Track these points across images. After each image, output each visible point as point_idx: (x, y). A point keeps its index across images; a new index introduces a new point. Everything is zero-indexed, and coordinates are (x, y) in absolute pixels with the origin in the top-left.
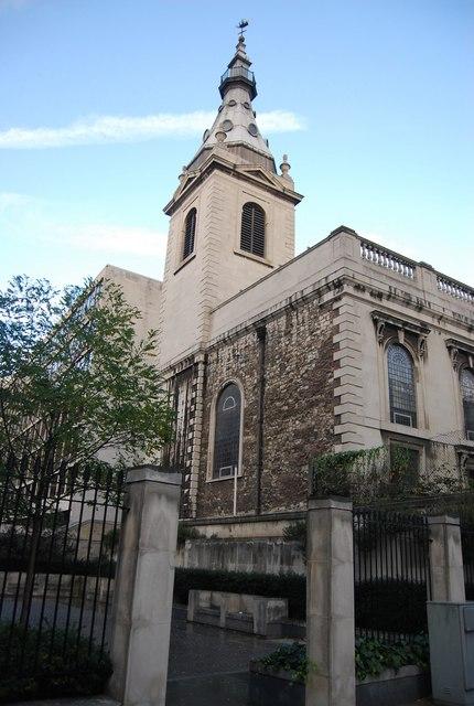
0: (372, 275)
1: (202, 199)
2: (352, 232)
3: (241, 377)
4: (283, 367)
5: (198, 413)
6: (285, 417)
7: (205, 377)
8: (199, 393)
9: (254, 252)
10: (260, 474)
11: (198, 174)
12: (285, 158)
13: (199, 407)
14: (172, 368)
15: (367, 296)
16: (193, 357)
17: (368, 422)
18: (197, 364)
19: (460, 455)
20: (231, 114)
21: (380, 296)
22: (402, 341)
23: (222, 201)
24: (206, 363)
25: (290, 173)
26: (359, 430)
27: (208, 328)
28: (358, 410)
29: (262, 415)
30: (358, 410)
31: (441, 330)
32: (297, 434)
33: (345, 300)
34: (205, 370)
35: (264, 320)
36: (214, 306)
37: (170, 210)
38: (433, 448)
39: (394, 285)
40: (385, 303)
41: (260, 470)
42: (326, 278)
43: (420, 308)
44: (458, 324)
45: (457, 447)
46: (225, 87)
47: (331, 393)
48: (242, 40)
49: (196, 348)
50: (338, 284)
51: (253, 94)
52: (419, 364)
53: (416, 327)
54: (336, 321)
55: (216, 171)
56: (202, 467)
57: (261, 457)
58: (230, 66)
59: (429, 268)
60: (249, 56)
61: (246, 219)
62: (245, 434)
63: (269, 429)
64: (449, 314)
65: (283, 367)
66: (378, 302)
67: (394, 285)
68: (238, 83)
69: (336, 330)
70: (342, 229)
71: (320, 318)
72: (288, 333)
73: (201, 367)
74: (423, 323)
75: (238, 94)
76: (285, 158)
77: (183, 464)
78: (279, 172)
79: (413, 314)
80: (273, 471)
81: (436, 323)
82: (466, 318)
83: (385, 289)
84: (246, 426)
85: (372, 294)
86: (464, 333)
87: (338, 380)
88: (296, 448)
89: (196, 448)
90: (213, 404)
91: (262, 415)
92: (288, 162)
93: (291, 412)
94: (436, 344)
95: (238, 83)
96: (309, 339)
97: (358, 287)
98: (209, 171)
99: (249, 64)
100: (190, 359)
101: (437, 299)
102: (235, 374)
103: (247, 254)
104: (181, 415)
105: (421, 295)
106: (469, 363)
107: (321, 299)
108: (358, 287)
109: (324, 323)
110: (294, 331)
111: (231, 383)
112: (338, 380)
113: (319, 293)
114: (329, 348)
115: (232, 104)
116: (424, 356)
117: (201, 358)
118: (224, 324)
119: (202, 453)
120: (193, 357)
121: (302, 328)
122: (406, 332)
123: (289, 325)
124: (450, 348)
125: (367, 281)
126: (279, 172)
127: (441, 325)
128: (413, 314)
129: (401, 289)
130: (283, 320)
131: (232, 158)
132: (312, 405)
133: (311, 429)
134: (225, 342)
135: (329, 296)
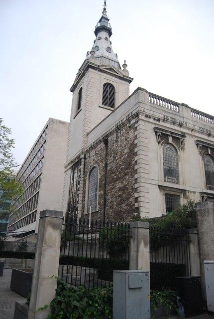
0: (155, 110)
1: (84, 84)
2: (144, 90)
3: (98, 164)
4: (115, 157)
5: (82, 182)
6: (115, 182)
7: (84, 165)
8: (82, 172)
9: (109, 106)
10: (105, 210)
11: (83, 72)
12: (125, 61)
13: (82, 179)
14: (72, 162)
15: (152, 120)
16: (80, 156)
17: (151, 182)
18: (81, 159)
19: (203, 197)
20: (99, 43)
21: (159, 120)
22: (170, 141)
23: (95, 82)
24: (85, 158)
25: (127, 68)
26: (146, 186)
27: (85, 142)
28: (146, 176)
29: (106, 181)
30: (146, 176)
32: (120, 189)
33: (140, 122)
34: (84, 162)
35: (107, 136)
36: (88, 132)
37: (72, 90)
38: (187, 194)
39: (166, 114)
40: (161, 123)
41: (105, 207)
42: (132, 113)
43: (181, 125)
44: (202, 132)
46: (97, 31)
47: (134, 168)
48: (105, 9)
49: (81, 151)
50: (137, 115)
51: (110, 34)
52: (180, 153)
53: (178, 135)
54: (136, 133)
55: (90, 69)
56: (83, 207)
57: (105, 201)
58: (100, 22)
59: (187, 106)
60: (108, 15)
61: (105, 91)
62: (100, 191)
63: (108, 187)
64: (197, 128)
65: (115, 157)
66: (158, 123)
67: (166, 114)
68: (103, 29)
69: (136, 137)
70: (139, 89)
71: (130, 132)
72: (117, 141)
73: (83, 160)
74: (182, 133)
75: (103, 34)
76: (125, 61)
78: (122, 68)
79: (176, 128)
80: (110, 208)
81: (190, 132)
82: (207, 130)
83: (161, 116)
84: (100, 187)
85: (154, 119)
86: (206, 137)
87: (137, 161)
88: (119, 196)
89: (80, 199)
90: (88, 177)
91: (106, 181)
92: (126, 63)
93: (118, 179)
94: (190, 143)
95: (103, 29)
96: (125, 143)
98: (87, 69)
99: (108, 20)
100: (79, 157)
101: (190, 119)
102: (96, 162)
103: (106, 107)
104: (75, 183)
105: (182, 119)
106: (208, 152)
107: (130, 123)
108: (146, 116)
110: (119, 140)
111: (94, 167)
112: (137, 161)
113: (129, 120)
114: (134, 146)
115: (100, 38)
117: (83, 156)
118: (92, 139)
119: (83, 201)
120: (80, 156)
121: (122, 138)
122: (173, 137)
123: (117, 137)
124: (197, 145)
125: (152, 112)
126: (122, 68)
127: (193, 133)
128: (176, 128)
129: (170, 116)
130: (115, 135)
131: (97, 62)
132: (126, 174)
133: (125, 186)
134: (92, 148)
135: (133, 121)
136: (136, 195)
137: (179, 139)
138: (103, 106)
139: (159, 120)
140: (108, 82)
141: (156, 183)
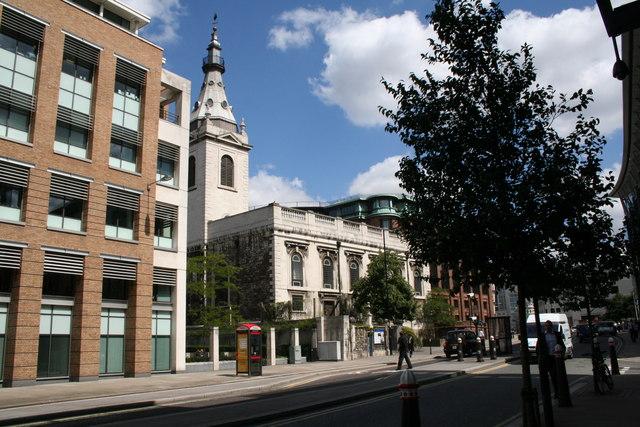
2: (277, 205)
15: (283, 234)
21: (289, 232)
31: (315, 242)
39: (294, 225)
40: (291, 235)
43: (306, 234)
45: (320, 294)
64: (319, 234)
67: (294, 225)
72: (249, 245)
77: (198, 299)
81: (313, 239)
83: (291, 229)
94: (312, 249)
97: (280, 230)
108: (280, 230)
109: (265, 245)
116: (307, 255)
127: (316, 239)
129: (297, 227)
132: (261, 279)
136: (271, 298)
137: (303, 248)
138: (222, 186)
139: (289, 232)
140: (226, 153)
141: (286, 287)
